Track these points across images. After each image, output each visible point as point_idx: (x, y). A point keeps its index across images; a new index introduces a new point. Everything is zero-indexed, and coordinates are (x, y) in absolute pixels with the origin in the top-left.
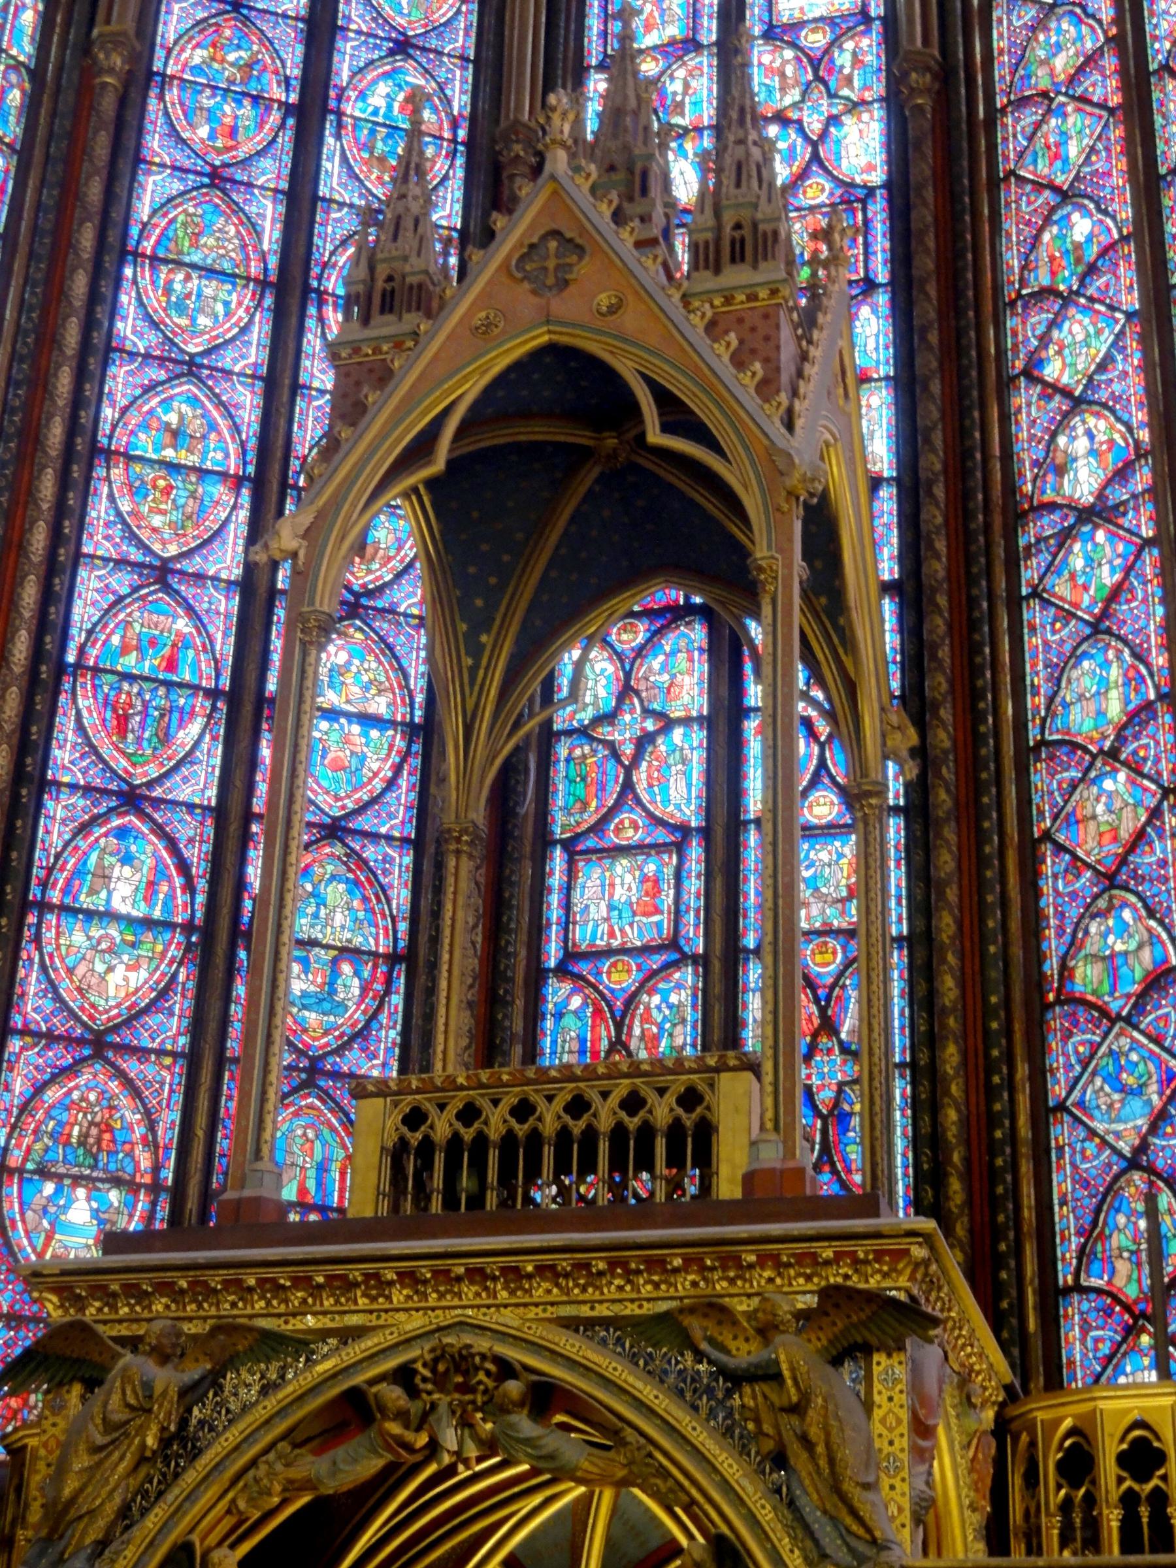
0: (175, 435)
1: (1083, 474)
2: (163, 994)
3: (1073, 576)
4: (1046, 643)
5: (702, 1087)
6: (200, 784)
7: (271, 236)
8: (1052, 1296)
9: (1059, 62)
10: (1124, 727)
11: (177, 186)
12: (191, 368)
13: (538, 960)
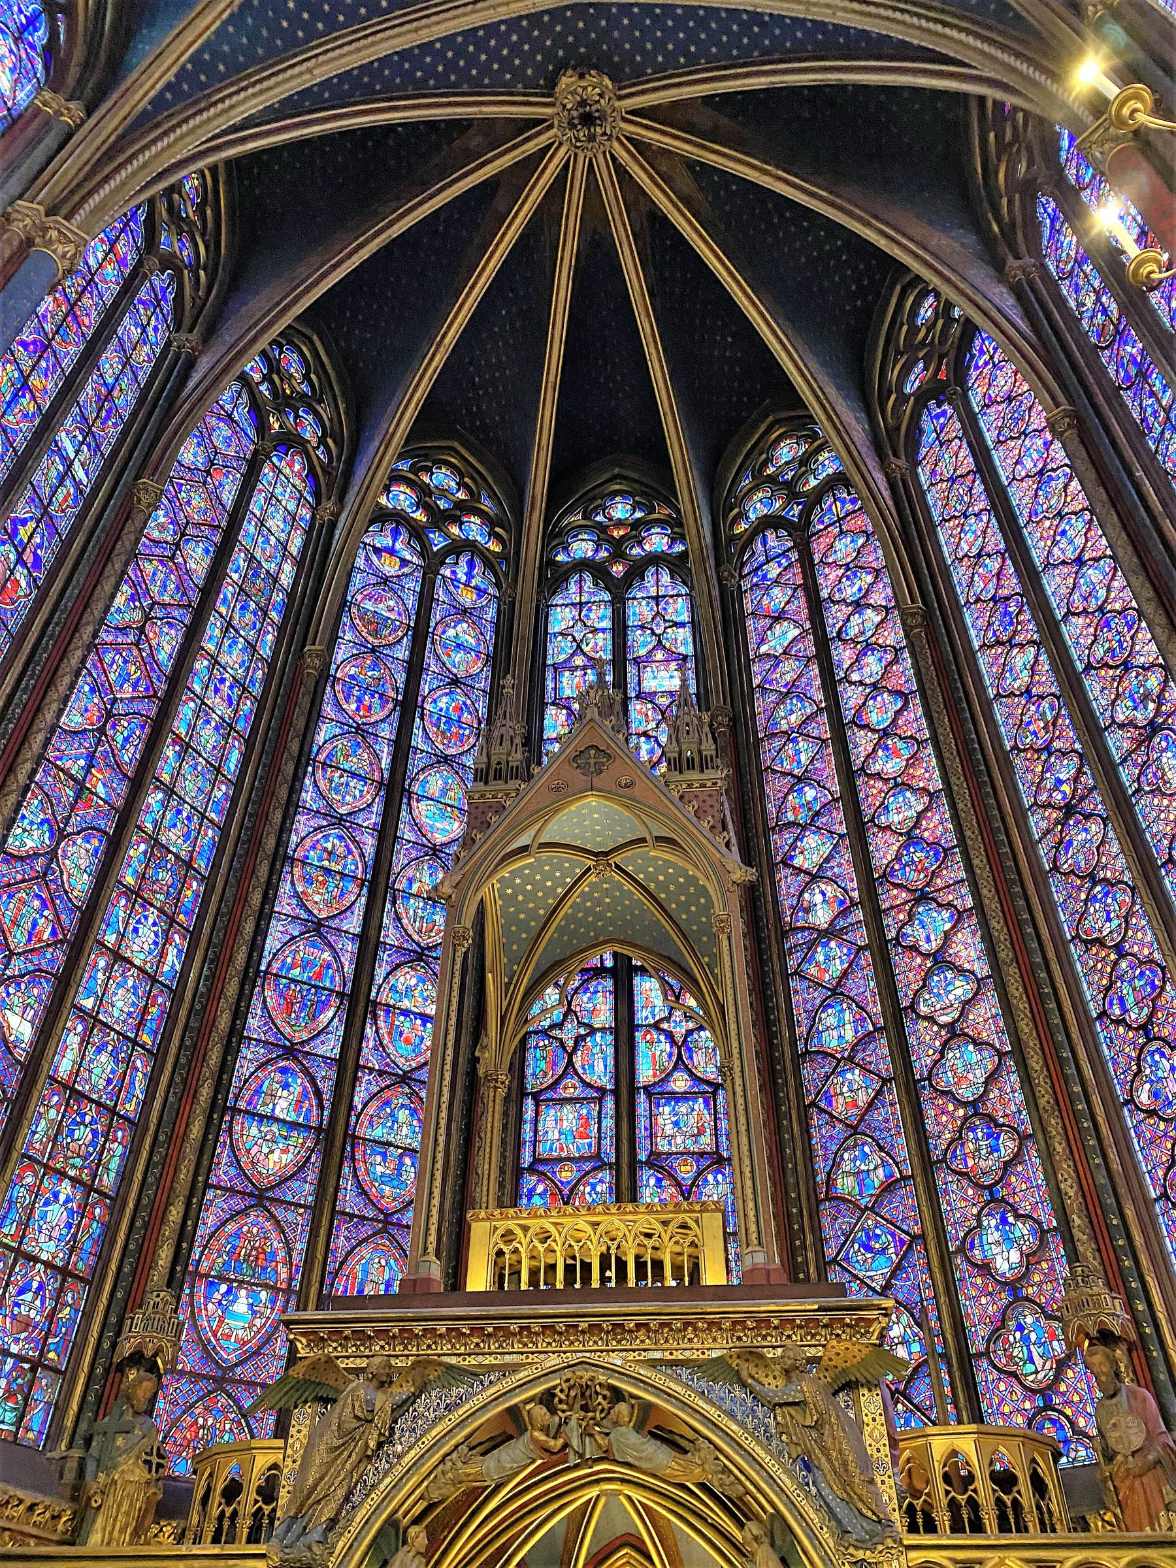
0: (330, 853)
1: (820, 913)
2: (301, 1169)
3: (818, 965)
5: (692, 1224)
6: (330, 1047)
7: (386, 761)
9: (793, 718)
10: (856, 1045)
11: (338, 731)
12: (340, 821)
13: (518, 1163)
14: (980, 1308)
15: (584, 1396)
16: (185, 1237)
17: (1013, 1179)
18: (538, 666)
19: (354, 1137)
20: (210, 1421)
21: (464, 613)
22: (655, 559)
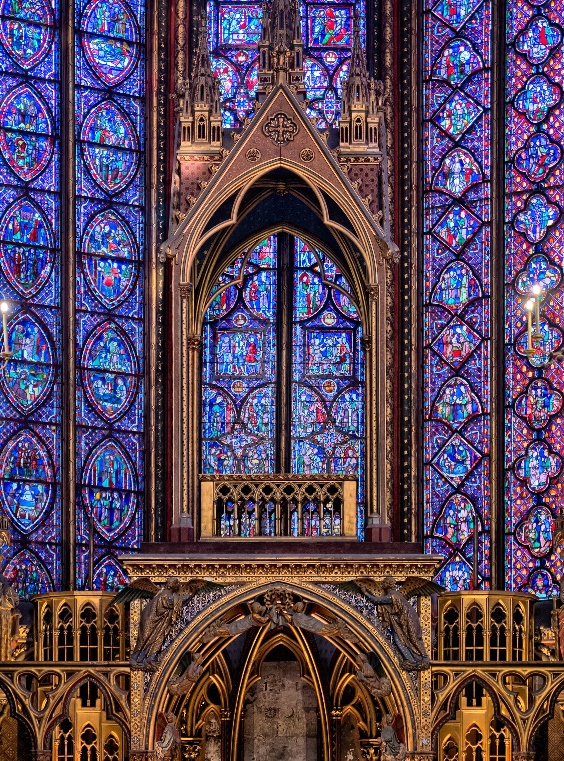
2: (49, 397)
4: (434, 259)
10: (467, 306)
17: (553, 428)
20: (24, 567)
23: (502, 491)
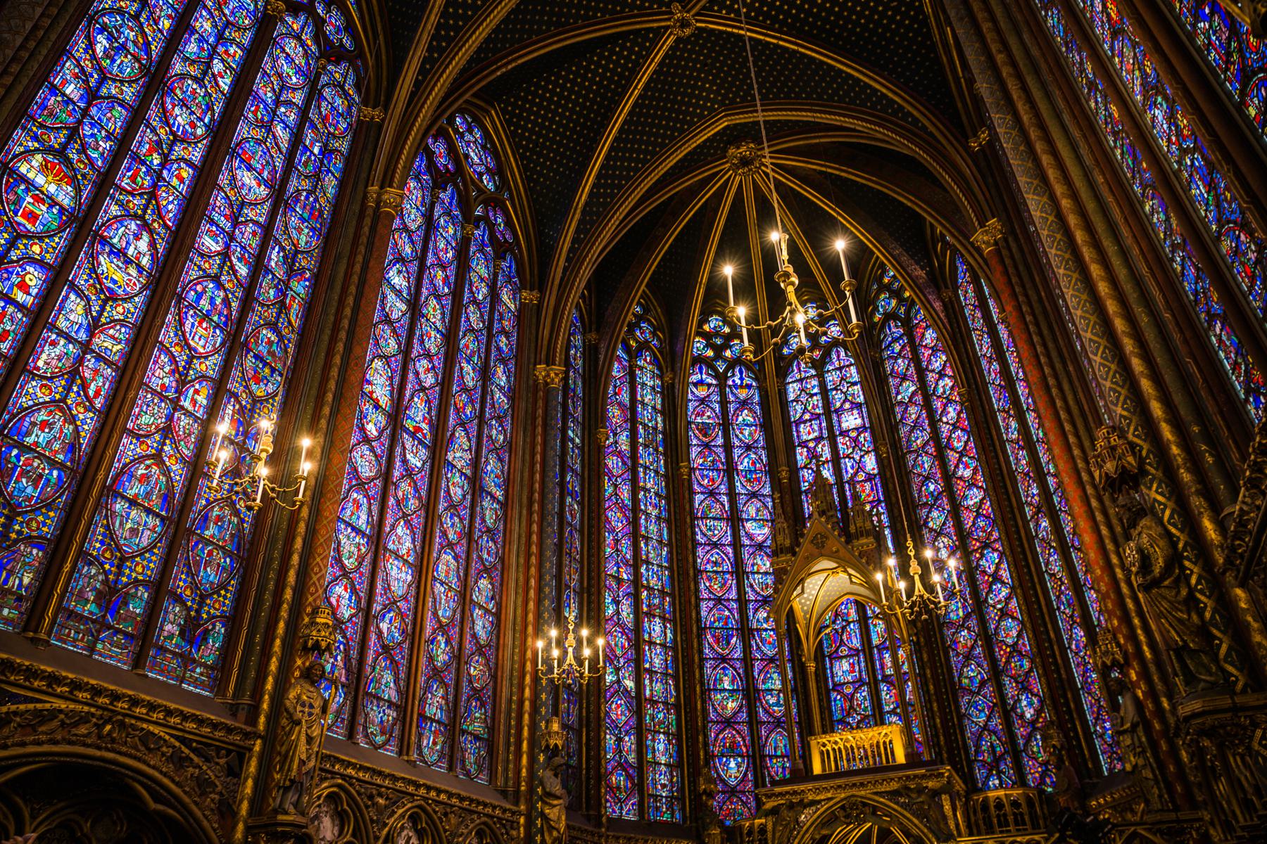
0: (715, 563)
6: (738, 654)
8: (970, 763)
11: (702, 497)
12: (715, 545)
14: (1021, 731)
15: (854, 806)
16: (706, 744)
18: (787, 424)
19: (757, 691)
21: (744, 404)
22: (836, 343)
23: (1008, 724)
